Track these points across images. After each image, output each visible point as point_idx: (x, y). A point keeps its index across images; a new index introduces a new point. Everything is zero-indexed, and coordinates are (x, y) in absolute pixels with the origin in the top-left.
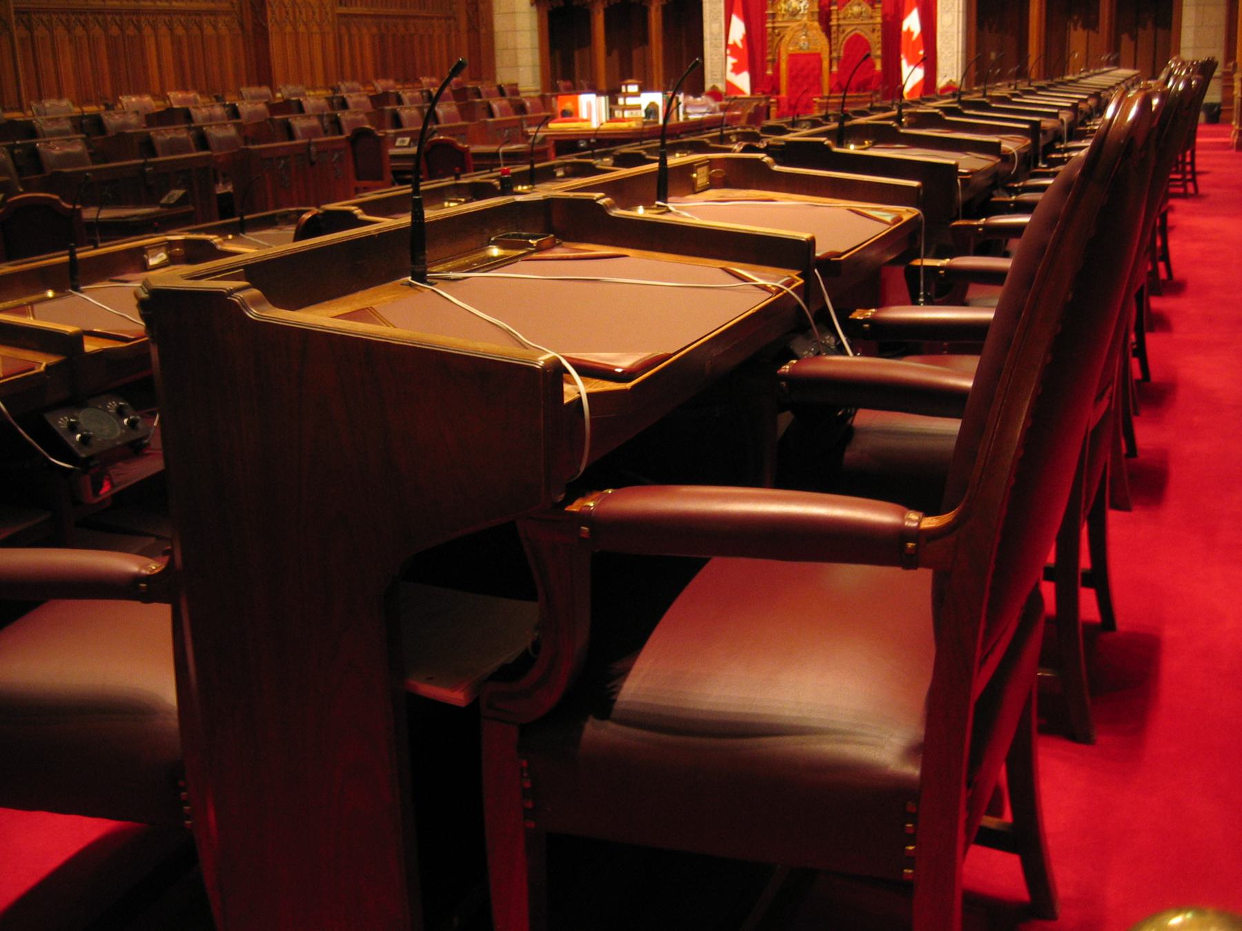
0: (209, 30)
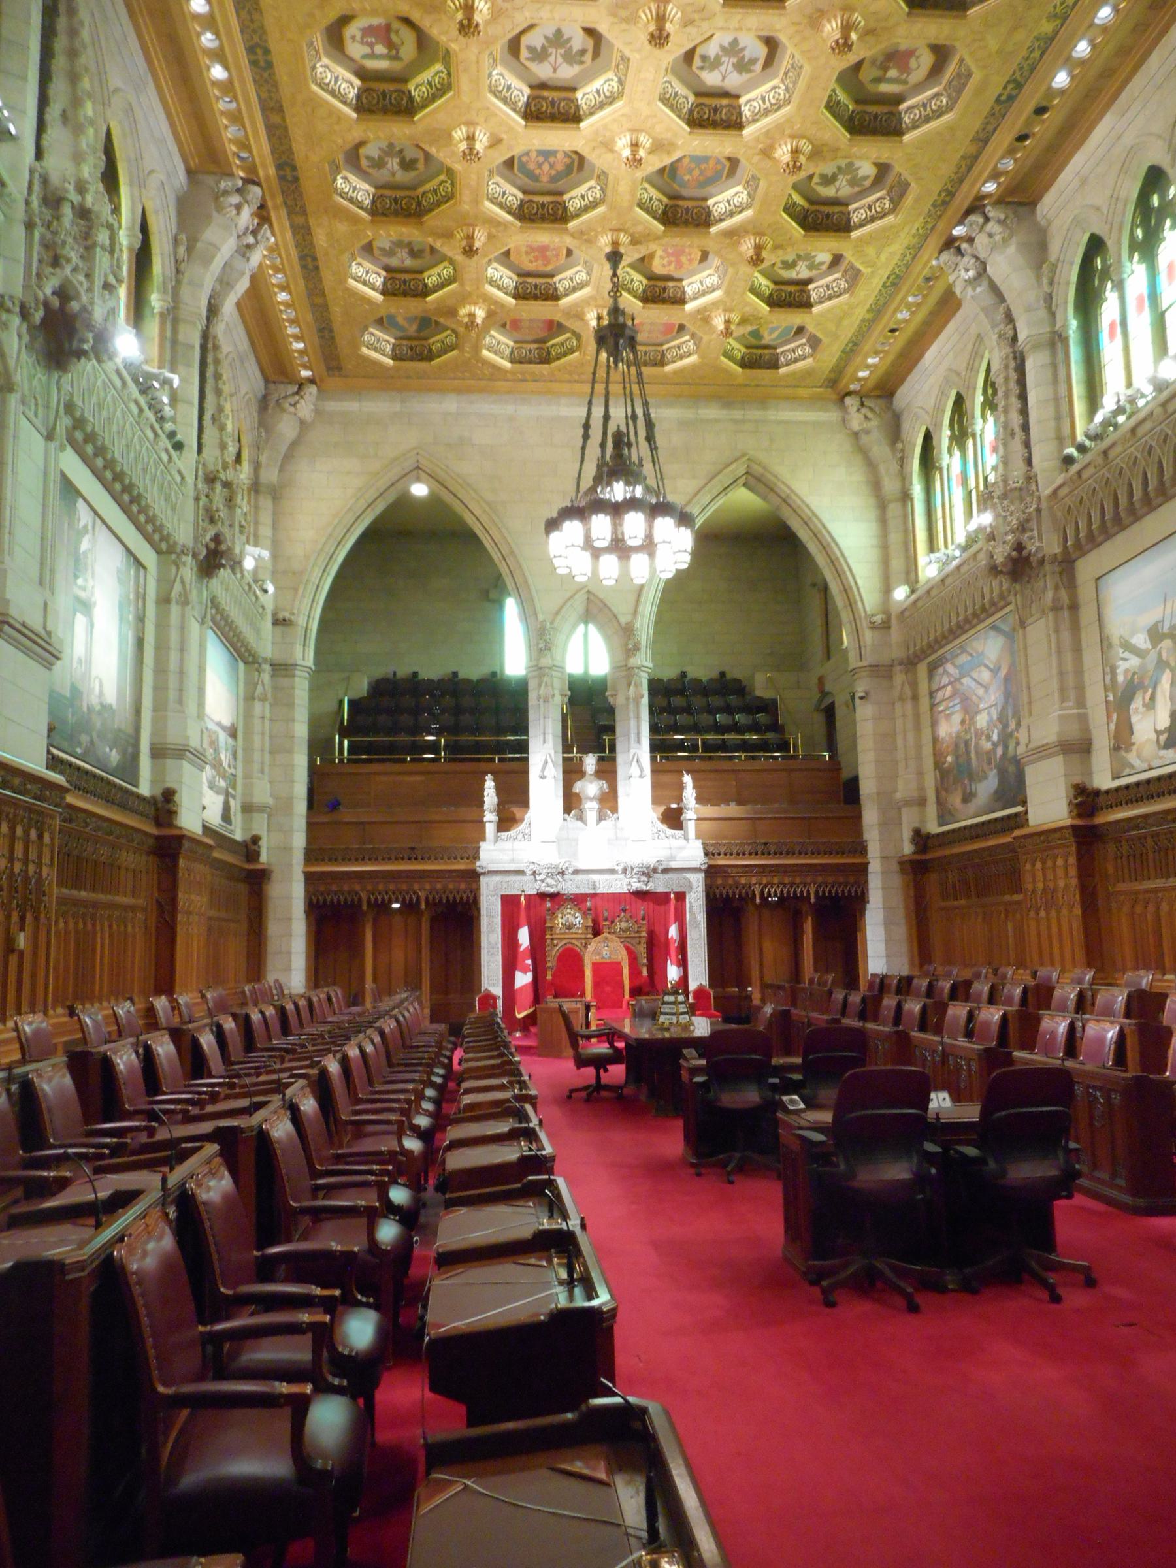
0: (130, 929)
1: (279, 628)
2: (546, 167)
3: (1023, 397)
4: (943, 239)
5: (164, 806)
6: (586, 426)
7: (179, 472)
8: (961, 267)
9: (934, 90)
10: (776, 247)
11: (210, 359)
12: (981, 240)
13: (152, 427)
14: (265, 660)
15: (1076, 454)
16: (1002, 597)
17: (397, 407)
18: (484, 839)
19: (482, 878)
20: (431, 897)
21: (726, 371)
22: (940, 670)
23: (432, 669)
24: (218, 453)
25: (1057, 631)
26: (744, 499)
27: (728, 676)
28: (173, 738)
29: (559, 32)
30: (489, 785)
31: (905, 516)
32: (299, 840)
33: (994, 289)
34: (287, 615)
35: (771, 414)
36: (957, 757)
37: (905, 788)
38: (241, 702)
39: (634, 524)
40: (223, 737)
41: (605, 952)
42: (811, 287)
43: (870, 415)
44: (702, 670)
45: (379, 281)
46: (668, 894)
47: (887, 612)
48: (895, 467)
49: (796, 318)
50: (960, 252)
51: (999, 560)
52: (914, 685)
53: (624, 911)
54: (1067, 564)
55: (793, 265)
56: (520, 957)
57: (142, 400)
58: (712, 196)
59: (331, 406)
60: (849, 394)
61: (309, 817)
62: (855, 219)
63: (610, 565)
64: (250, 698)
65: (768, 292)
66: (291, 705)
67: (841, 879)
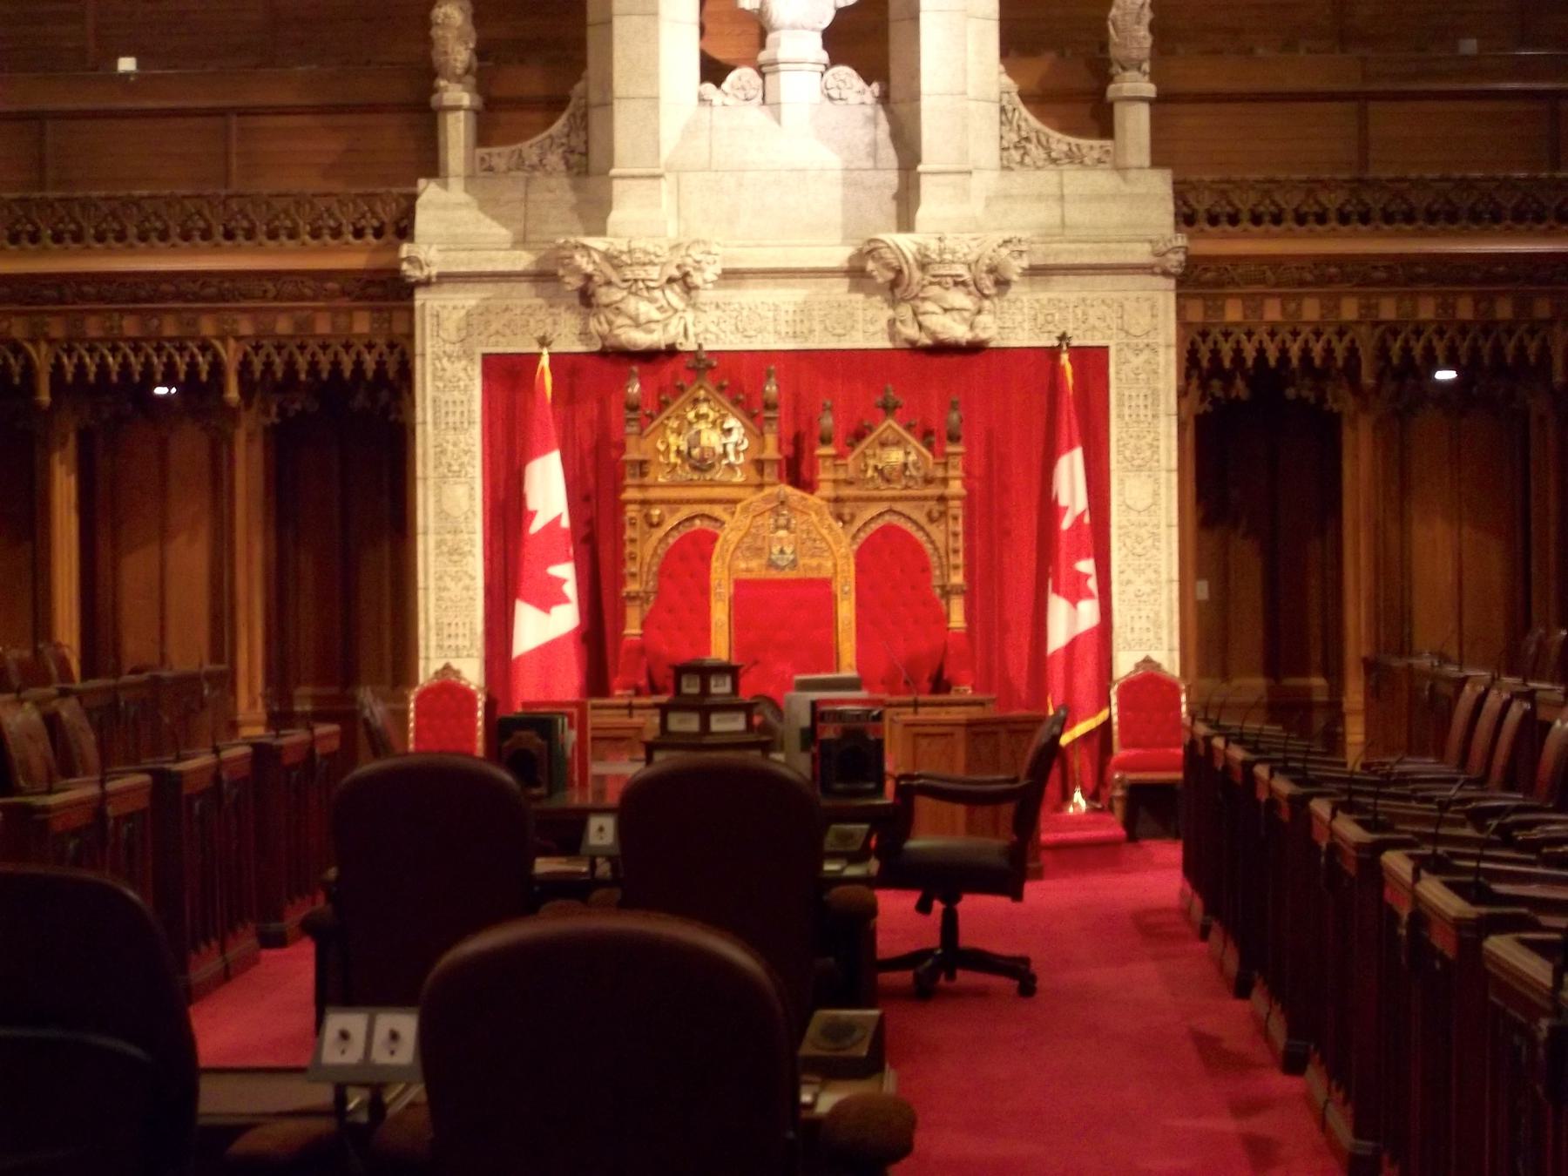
18: (432, 167)
19: (420, 297)
20: (257, 365)
41: (783, 545)
53: (888, 409)
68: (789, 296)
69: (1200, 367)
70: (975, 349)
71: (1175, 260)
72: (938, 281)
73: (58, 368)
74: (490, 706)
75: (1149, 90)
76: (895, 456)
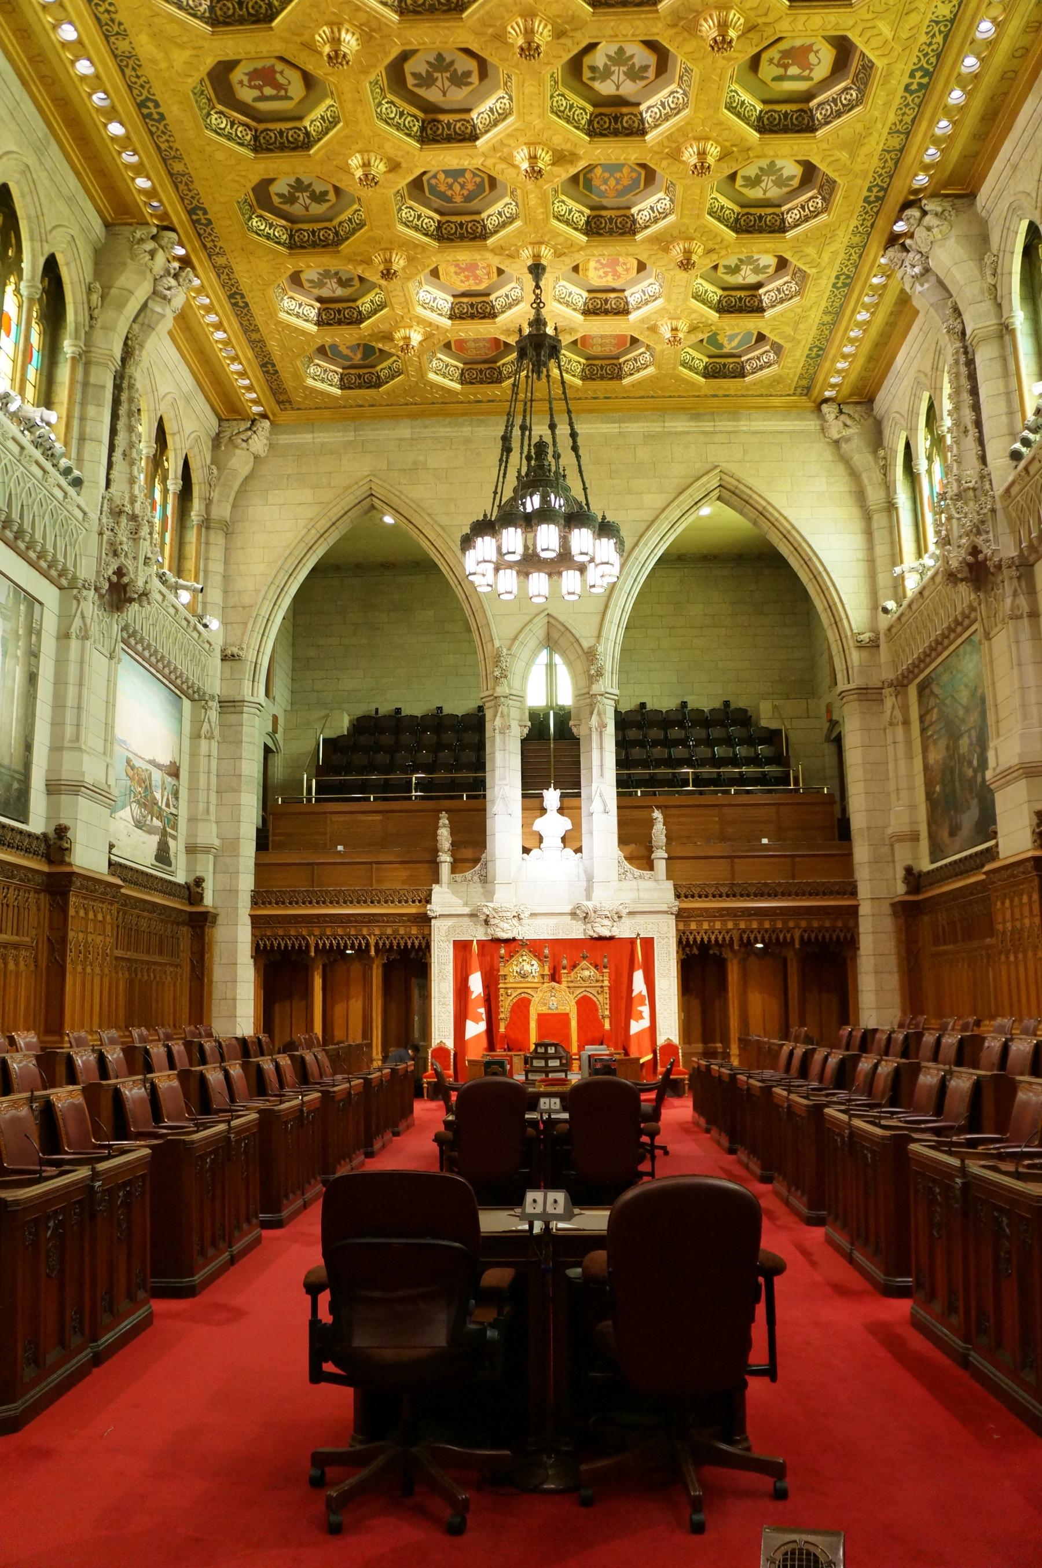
0: (11, 966)
1: (228, 664)
2: (457, 187)
3: (974, 392)
4: (886, 236)
5: (56, 844)
6: (506, 439)
7: (79, 507)
8: (907, 263)
9: (843, 85)
10: (709, 251)
11: (124, 397)
12: (920, 233)
13: (37, 463)
14: (212, 697)
15: (1024, 450)
16: (973, 609)
17: (350, 436)
18: (437, 880)
19: (433, 922)
21: (692, 384)
22: (927, 691)
23: (416, 705)
24: (125, 487)
25: (1017, 642)
26: (713, 515)
27: (733, 706)
28: (67, 774)
29: (440, 57)
30: (444, 820)
31: (891, 528)
32: (246, 882)
33: (941, 283)
34: (235, 650)
35: (744, 425)
36: (944, 785)
37: (898, 821)
38: (186, 741)
39: (548, 537)
40: (157, 776)
42: (761, 291)
43: (849, 422)
44: (704, 699)
45: (313, 314)
46: (632, 942)
47: (874, 630)
48: (877, 475)
49: (750, 324)
50: (905, 249)
51: (954, 564)
52: (905, 708)
54: (1025, 568)
55: (735, 270)
56: (471, 1007)
57: (26, 439)
58: (635, 204)
59: (284, 439)
60: (826, 401)
61: (256, 858)
62: (789, 219)
63: (539, 582)
64: (196, 736)
65: (716, 298)
66: (238, 743)
67: (827, 924)
68: (552, 921)
69: (682, 943)
70: (612, 938)
71: (675, 910)
72: (600, 916)
73: (317, 944)
74: (455, 1055)
75: (666, 855)
76: (586, 973)
